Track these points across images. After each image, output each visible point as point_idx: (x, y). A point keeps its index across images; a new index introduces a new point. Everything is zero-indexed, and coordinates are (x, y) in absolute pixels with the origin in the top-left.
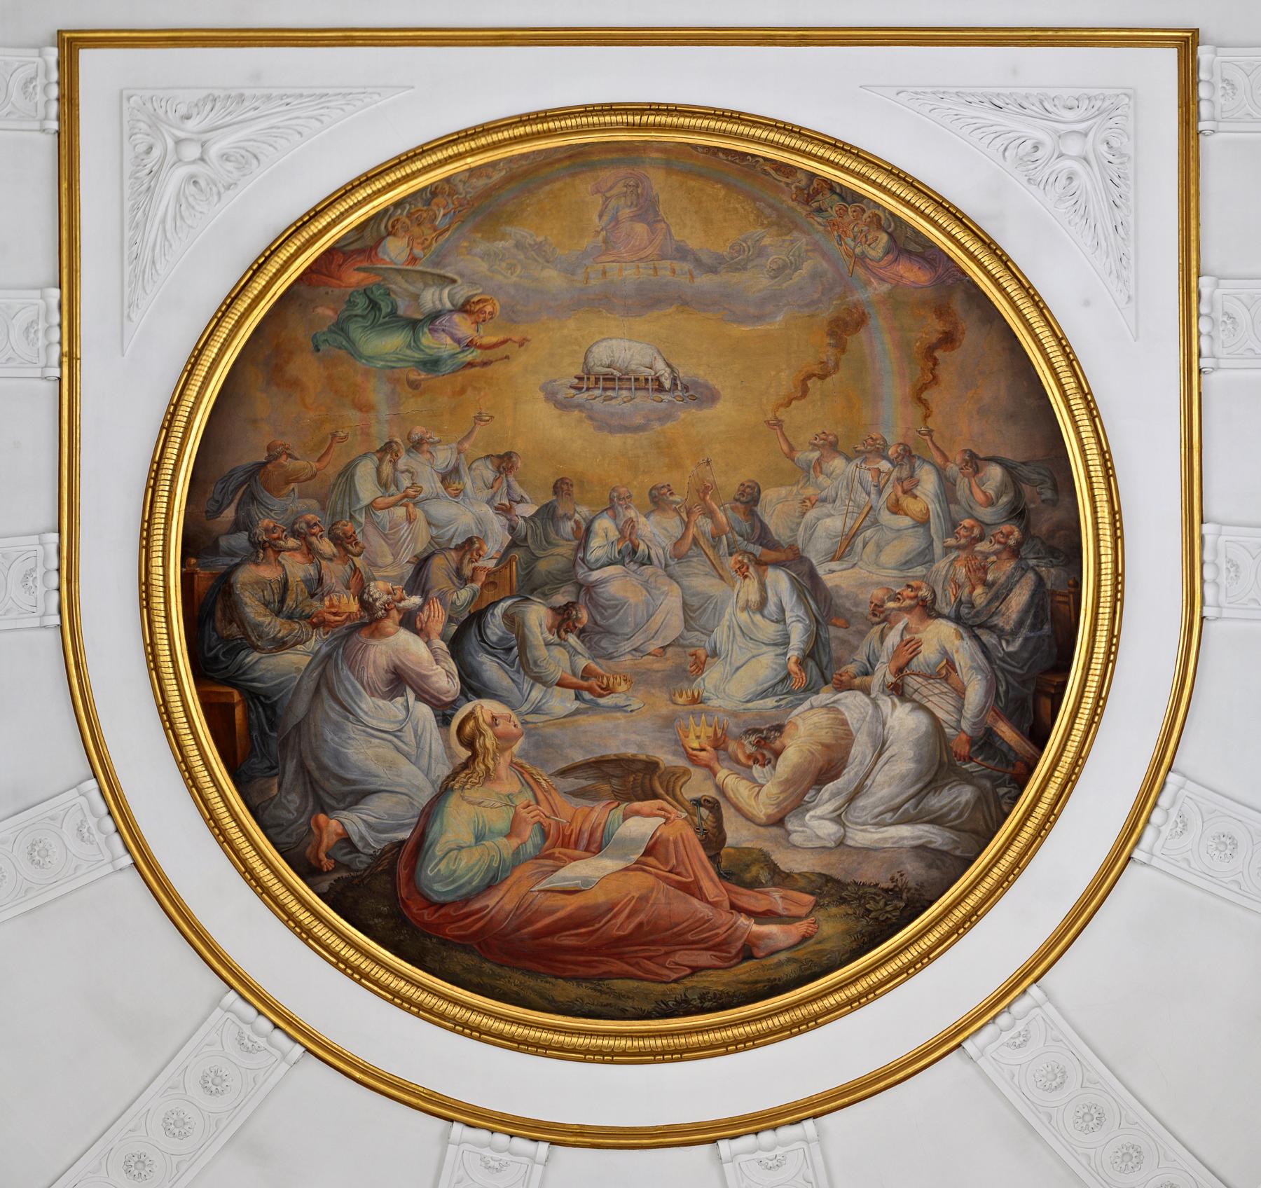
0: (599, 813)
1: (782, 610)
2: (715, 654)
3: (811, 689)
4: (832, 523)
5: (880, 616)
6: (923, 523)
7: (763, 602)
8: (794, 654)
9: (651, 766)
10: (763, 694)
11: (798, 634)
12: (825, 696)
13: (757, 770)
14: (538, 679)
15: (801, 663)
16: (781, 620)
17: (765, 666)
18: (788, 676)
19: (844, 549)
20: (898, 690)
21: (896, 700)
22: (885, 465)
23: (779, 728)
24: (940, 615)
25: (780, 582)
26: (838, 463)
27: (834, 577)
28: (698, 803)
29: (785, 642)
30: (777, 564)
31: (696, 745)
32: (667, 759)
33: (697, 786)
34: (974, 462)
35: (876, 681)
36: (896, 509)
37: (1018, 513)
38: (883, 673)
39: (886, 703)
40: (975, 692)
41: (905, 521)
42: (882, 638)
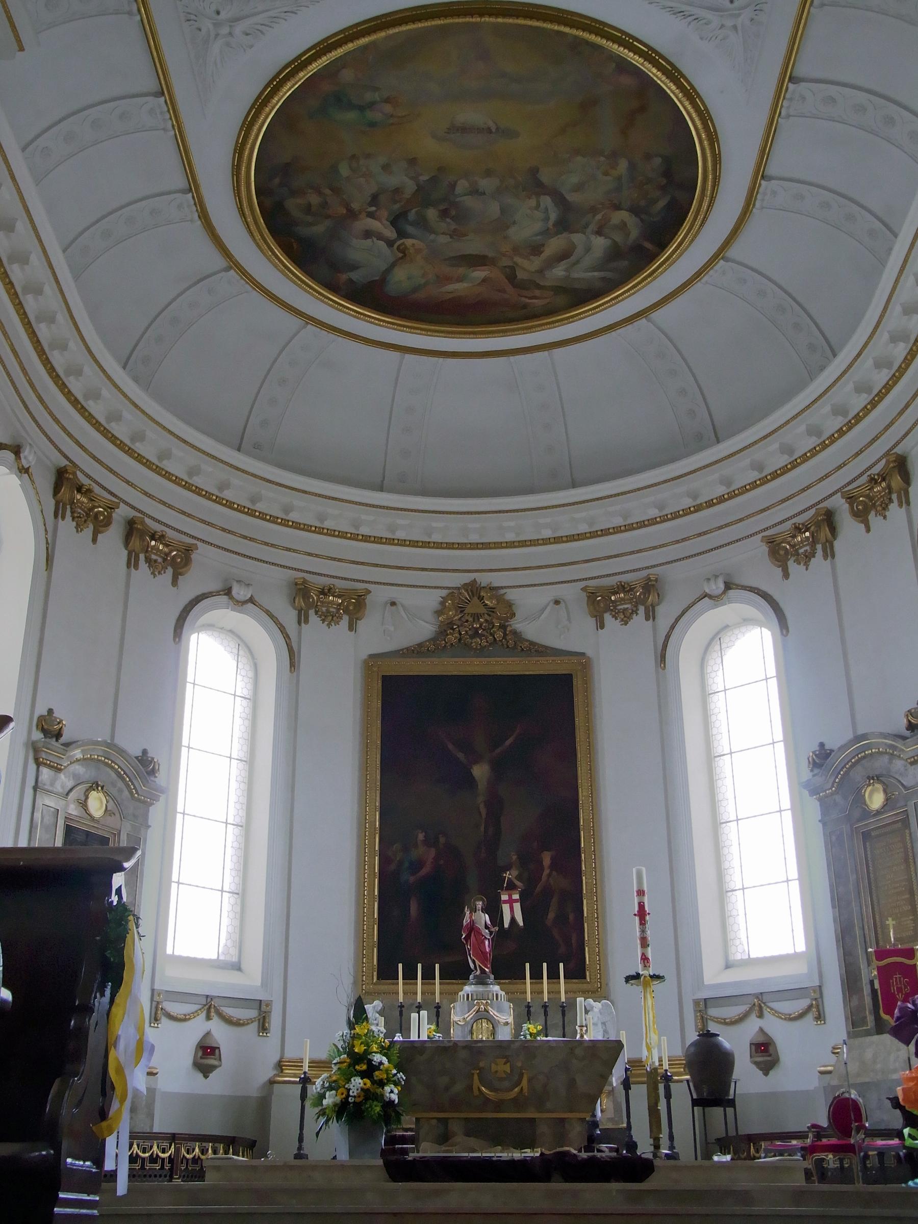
0: (461, 270)
1: (547, 209)
2: (514, 223)
3: (557, 234)
4: (574, 179)
5: (593, 210)
6: (619, 178)
7: (538, 205)
8: (551, 223)
9: (484, 257)
10: (537, 235)
11: (553, 216)
12: (565, 235)
13: (532, 257)
14: (434, 233)
15: (554, 225)
16: (546, 210)
17: (538, 226)
18: (548, 229)
19: (579, 188)
20: (599, 233)
21: (597, 236)
22: (602, 159)
23: (543, 245)
24: (622, 210)
25: (546, 201)
26: (579, 158)
27: (571, 197)
28: (505, 267)
29: (547, 219)
30: (545, 194)
31: (505, 250)
32: (491, 254)
33: (505, 262)
34: (648, 157)
35: (589, 230)
36: (606, 174)
37: (667, 173)
38: (593, 227)
39: (593, 237)
40: (634, 233)
41: (609, 178)
42: (594, 216)
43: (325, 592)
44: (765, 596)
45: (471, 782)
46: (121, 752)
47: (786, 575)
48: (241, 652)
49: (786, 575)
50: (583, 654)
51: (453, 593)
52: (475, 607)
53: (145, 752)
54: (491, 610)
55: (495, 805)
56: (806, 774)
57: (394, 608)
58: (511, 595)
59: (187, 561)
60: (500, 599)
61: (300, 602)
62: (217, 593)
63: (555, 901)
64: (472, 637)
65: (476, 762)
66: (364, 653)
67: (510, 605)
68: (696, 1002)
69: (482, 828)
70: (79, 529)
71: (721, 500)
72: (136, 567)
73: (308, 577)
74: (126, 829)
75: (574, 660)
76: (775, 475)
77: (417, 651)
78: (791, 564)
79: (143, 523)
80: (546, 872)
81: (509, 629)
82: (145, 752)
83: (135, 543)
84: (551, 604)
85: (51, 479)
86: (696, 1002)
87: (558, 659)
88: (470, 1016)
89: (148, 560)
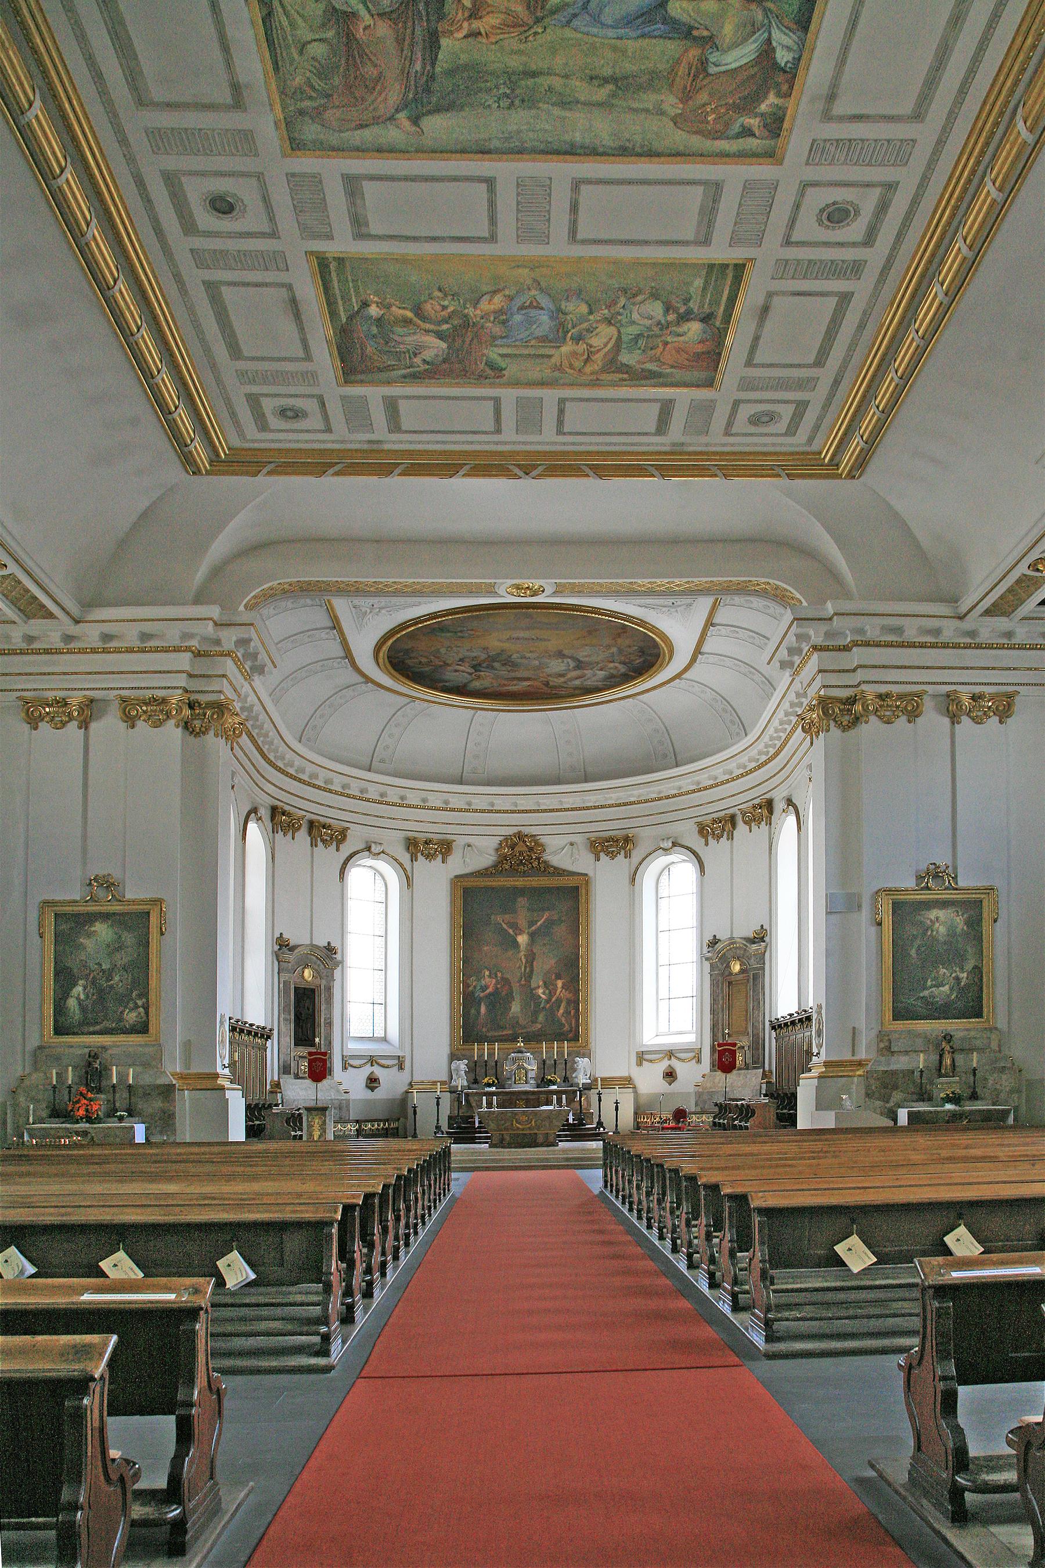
43: (427, 842)
44: (694, 853)
46: (317, 947)
47: (707, 844)
49: (707, 844)
53: (329, 943)
56: (705, 949)
59: (345, 836)
62: (362, 851)
64: (518, 865)
70: (285, 835)
71: (674, 796)
72: (316, 846)
73: (416, 835)
74: (324, 982)
76: (706, 789)
78: (710, 838)
79: (318, 822)
82: (329, 943)
83: (315, 831)
85: (269, 813)
88: (514, 1067)
89: (323, 841)
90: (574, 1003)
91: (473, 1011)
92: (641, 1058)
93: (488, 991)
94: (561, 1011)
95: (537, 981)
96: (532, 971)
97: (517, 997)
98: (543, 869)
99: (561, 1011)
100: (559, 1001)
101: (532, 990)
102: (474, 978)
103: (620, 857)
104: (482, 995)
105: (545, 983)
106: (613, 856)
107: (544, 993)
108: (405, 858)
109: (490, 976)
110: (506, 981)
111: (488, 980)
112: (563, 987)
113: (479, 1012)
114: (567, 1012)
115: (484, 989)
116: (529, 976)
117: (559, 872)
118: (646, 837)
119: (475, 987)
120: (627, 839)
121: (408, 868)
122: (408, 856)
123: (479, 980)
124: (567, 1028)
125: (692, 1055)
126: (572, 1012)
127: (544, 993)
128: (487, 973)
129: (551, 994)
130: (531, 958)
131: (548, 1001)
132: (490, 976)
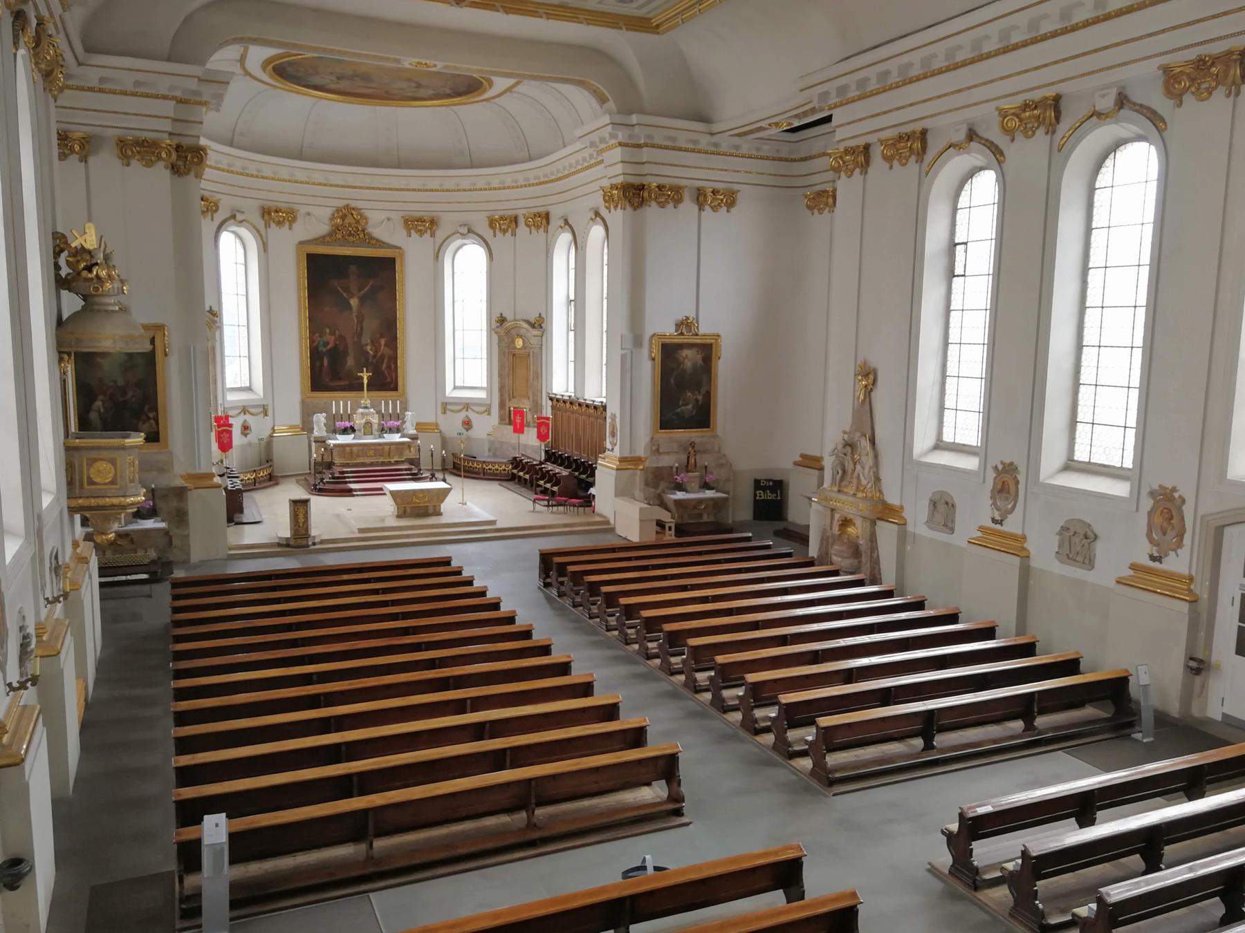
45: (349, 306)
48: (237, 240)
50: (400, 248)
51: (338, 210)
52: (349, 220)
54: (357, 222)
55: (361, 319)
57: (309, 217)
58: (367, 213)
60: (361, 215)
61: (266, 217)
63: (385, 361)
65: (352, 297)
66: (296, 242)
67: (366, 218)
68: (443, 403)
69: (355, 328)
75: (398, 250)
77: (321, 240)
80: (382, 347)
81: (366, 231)
84: (386, 221)
86: (443, 403)
87: (389, 250)
90: (394, 359)
91: (318, 364)
92: (446, 406)
93: (329, 347)
94: (384, 365)
95: (366, 339)
96: (362, 329)
97: (351, 351)
98: (367, 241)
99: (384, 365)
100: (383, 357)
101: (362, 346)
102: (317, 335)
103: (427, 235)
104: (324, 350)
105: (372, 341)
106: (421, 233)
107: (371, 350)
108: (260, 224)
109: (330, 334)
110: (342, 338)
111: (328, 337)
112: (385, 345)
113: (322, 365)
114: (389, 367)
115: (326, 344)
116: (360, 335)
117: (381, 244)
118: (448, 222)
119: (319, 343)
120: (433, 222)
121: (263, 234)
122: (262, 222)
123: (321, 336)
124: (389, 380)
125: (484, 409)
126: (393, 367)
127: (371, 350)
128: (328, 331)
129: (376, 352)
130: (361, 319)
131: (374, 357)
132: (330, 334)
